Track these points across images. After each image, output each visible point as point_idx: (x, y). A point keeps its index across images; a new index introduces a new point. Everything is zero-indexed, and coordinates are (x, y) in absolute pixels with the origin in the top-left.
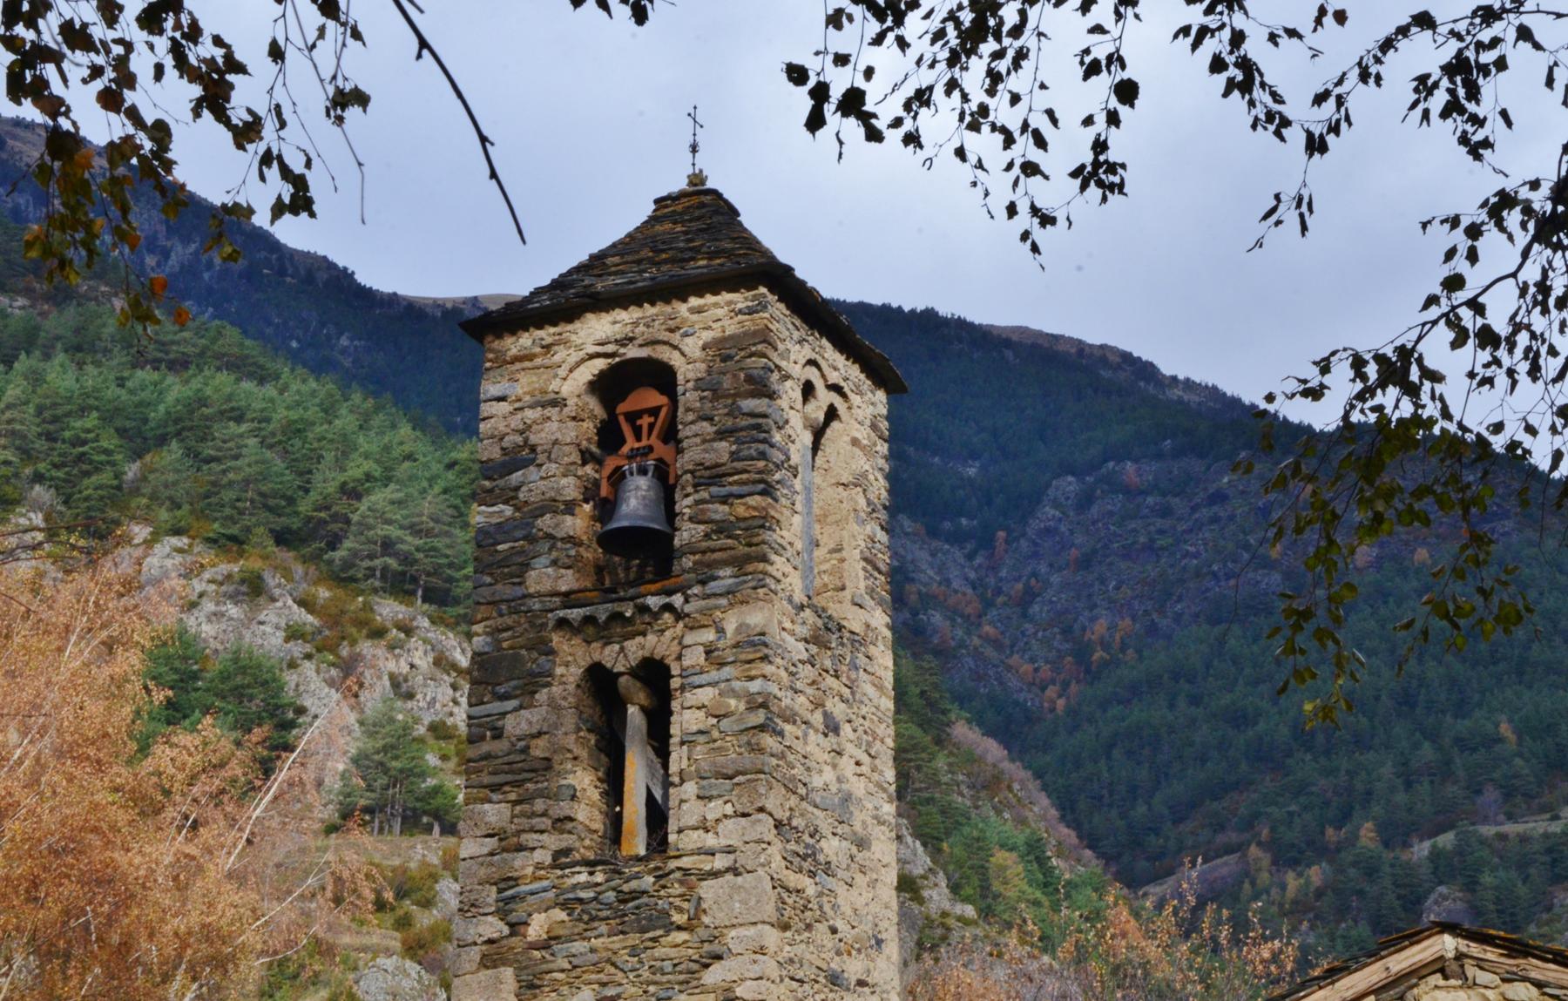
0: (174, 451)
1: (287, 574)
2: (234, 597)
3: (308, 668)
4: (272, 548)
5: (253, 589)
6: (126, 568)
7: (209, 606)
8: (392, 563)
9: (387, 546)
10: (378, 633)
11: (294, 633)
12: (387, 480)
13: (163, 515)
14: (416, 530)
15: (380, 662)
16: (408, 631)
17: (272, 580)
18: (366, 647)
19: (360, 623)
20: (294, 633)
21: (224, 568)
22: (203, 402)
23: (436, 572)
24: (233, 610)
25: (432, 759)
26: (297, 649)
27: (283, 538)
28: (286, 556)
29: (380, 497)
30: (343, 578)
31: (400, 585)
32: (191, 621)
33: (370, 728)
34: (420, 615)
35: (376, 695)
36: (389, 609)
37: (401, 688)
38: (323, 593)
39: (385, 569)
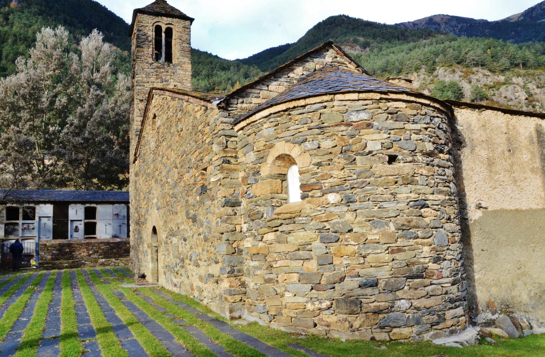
0: (441, 55)
1: (458, 68)
2: (451, 74)
3: (463, 81)
4: (457, 65)
5: (454, 71)
6: (436, 73)
7: (448, 76)
8: (475, 62)
9: (473, 60)
10: (473, 73)
11: (460, 77)
12: (473, 49)
13: (441, 65)
14: (477, 56)
15: (474, 78)
16: (478, 72)
17: (456, 70)
18: (472, 76)
19: (470, 72)
20: (460, 77)
21: (450, 69)
22: (445, 47)
23: (482, 62)
24: (451, 75)
25: (484, 90)
26: (461, 79)
27: (458, 63)
28: (459, 66)
29: (471, 53)
30: (467, 66)
31: (476, 65)
32: (446, 78)
33: (472, 87)
34: (479, 69)
35: (474, 81)
36: (475, 69)
37: (478, 81)
38: (464, 69)
39: (474, 64)
